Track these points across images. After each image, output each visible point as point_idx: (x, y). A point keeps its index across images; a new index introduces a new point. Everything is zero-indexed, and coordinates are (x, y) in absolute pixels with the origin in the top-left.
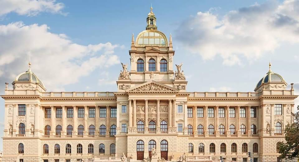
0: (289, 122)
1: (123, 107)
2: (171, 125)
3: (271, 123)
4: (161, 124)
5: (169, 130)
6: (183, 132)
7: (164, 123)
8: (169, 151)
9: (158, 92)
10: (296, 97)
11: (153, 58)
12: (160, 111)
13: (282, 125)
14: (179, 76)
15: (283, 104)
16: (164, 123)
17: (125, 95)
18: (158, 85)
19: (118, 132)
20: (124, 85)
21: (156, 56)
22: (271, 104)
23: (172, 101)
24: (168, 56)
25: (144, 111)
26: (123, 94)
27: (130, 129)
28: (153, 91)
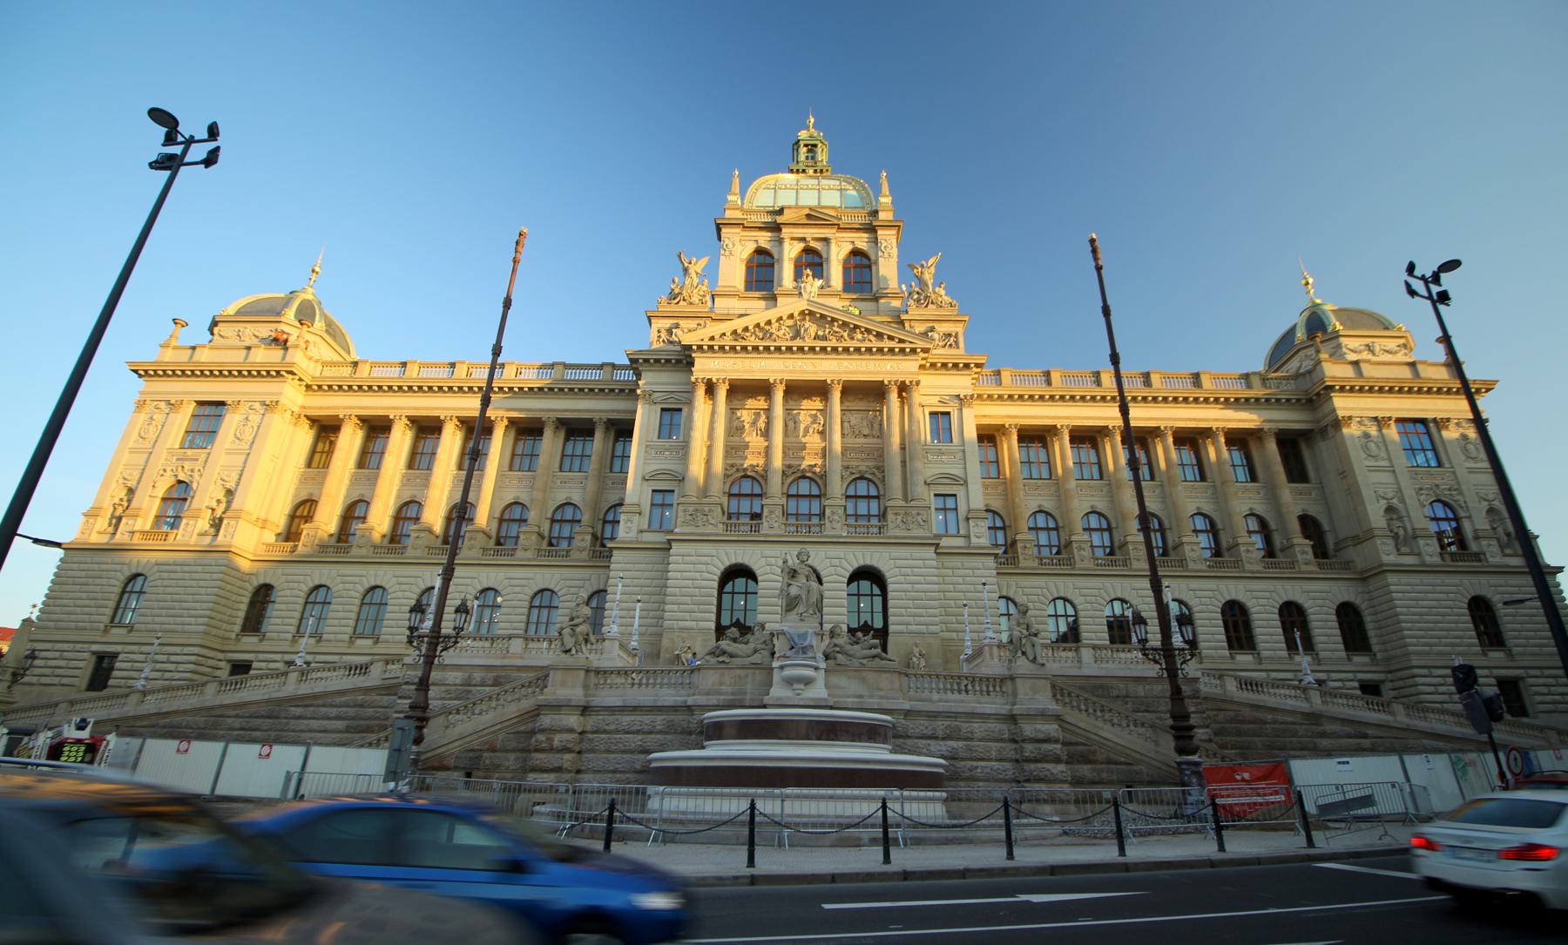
0: (1491, 497)
1: (667, 416)
2: (898, 493)
3: (1403, 501)
4: (851, 492)
5: (890, 517)
6: (962, 532)
7: (862, 488)
8: (892, 628)
9: (835, 349)
10: (1488, 390)
11: (813, 244)
12: (843, 435)
13: (1462, 514)
14: (927, 297)
15: (1435, 420)
16: (862, 488)
17: (678, 361)
18: (834, 320)
19: (627, 529)
20: (677, 326)
21: (826, 240)
22: (1376, 419)
23: (903, 388)
24: (876, 241)
25: (767, 433)
26: (668, 361)
27: (691, 509)
28: (808, 343)
